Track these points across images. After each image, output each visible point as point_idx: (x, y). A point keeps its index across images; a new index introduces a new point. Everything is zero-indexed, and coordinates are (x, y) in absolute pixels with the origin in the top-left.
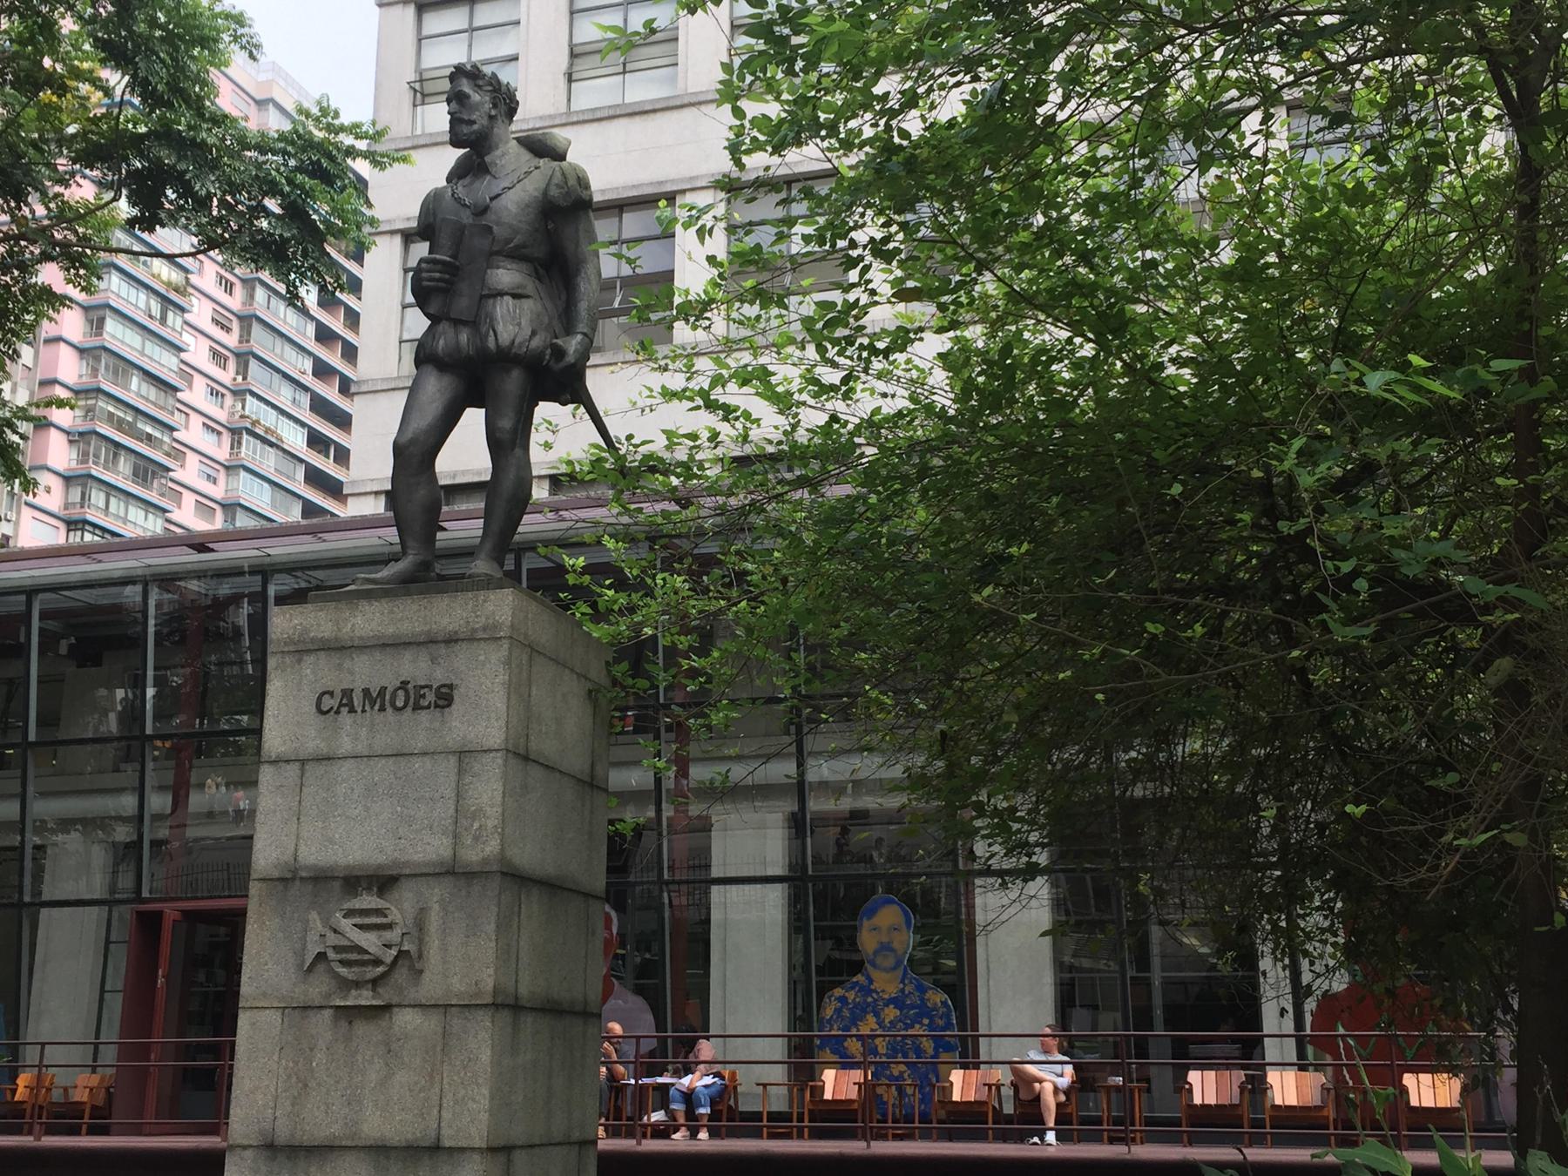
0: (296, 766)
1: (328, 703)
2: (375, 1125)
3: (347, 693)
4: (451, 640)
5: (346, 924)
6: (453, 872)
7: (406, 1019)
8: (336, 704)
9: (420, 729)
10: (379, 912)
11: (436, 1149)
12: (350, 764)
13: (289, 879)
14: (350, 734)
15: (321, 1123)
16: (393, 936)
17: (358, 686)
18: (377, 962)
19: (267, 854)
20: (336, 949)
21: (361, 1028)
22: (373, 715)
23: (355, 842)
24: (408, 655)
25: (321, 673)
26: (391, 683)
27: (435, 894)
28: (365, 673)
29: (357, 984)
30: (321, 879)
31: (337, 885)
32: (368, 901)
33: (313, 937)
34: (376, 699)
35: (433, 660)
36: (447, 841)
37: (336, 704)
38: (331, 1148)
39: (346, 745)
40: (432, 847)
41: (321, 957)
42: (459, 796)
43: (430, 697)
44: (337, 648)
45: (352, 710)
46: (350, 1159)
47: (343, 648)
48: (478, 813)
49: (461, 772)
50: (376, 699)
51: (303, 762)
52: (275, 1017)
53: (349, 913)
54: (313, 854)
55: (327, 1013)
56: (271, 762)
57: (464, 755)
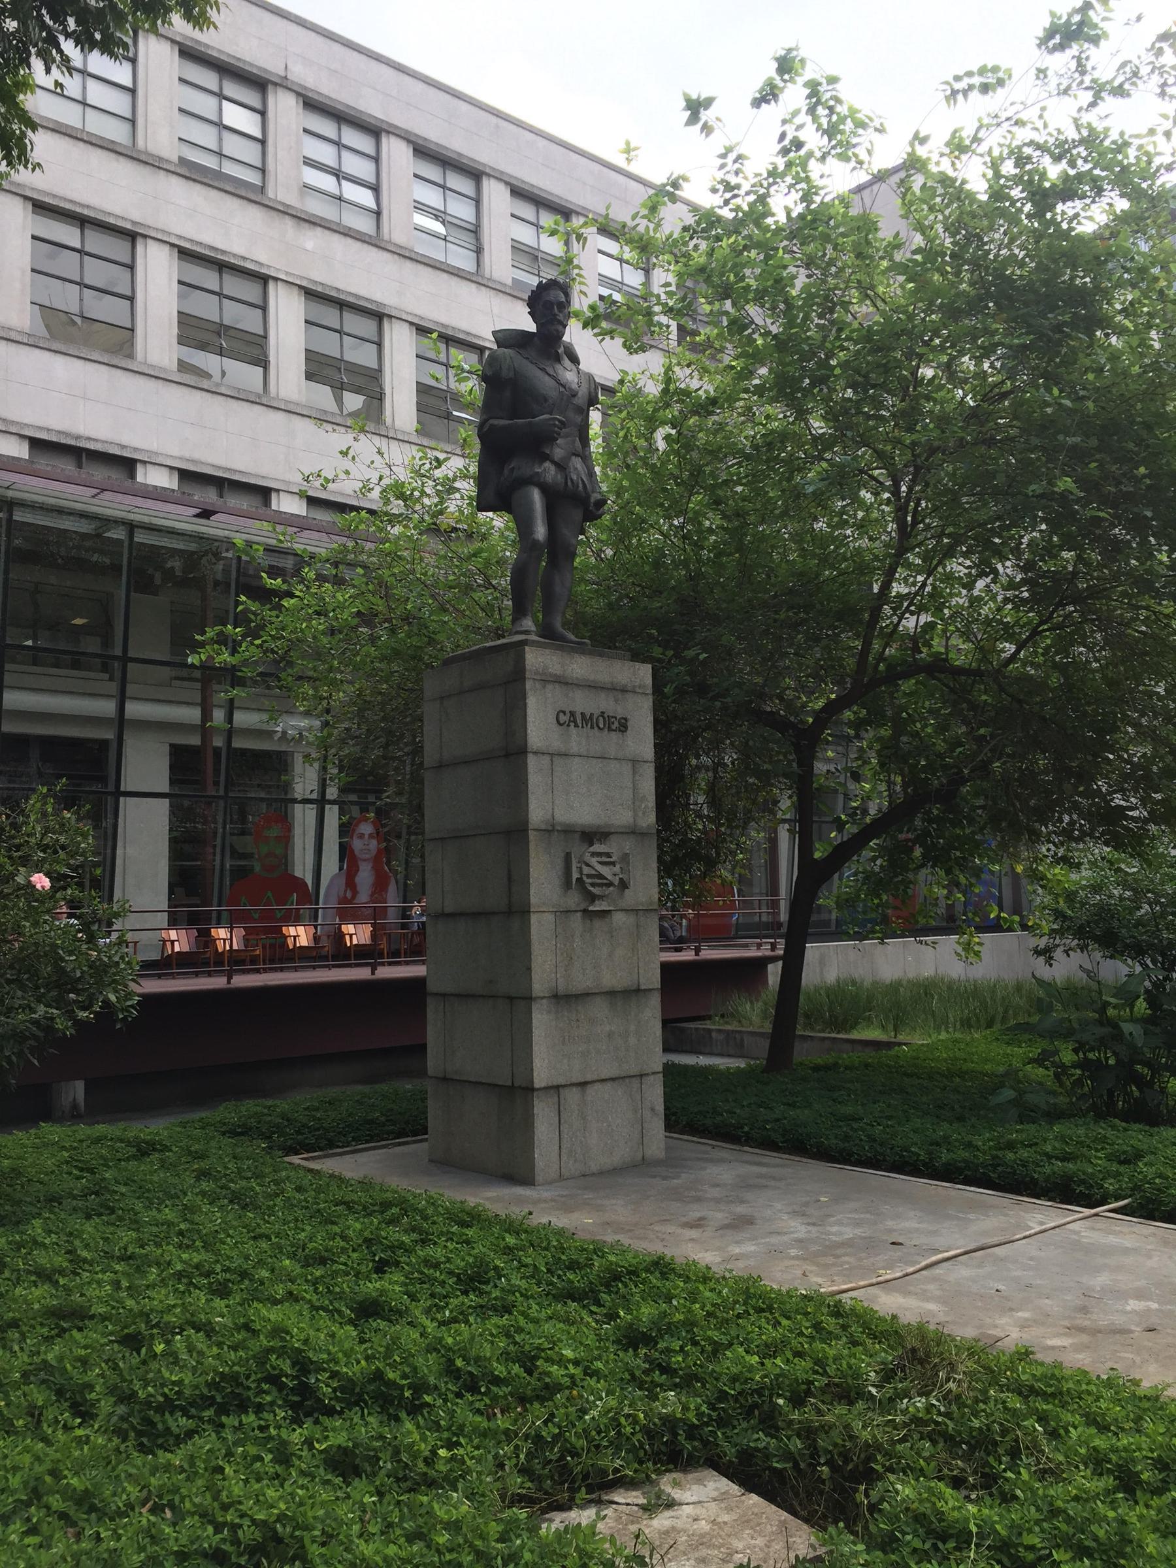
0: (547, 759)
1: (563, 718)
2: (610, 980)
3: (572, 714)
4: (624, 690)
5: (594, 861)
6: (633, 832)
7: (619, 918)
8: (568, 720)
9: (610, 742)
10: (608, 855)
11: (638, 991)
12: (577, 759)
13: (551, 830)
14: (577, 740)
15: (582, 981)
16: (617, 869)
17: (578, 710)
18: (610, 884)
19: (537, 813)
20: (589, 876)
21: (598, 923)
22: (587, 729)
23: (583, 810)
24: (603, 695)
25: (555, 698)
26: (596, 714)
27: (628, 845)
28: (582, 702)
29: (601, 897)
30: (568, 831)
31: (577, 836)
32: (597, 847)
33: (574, 869)
34: (588, 721)
35: (616, 701)
36: (631, 814)
37: (568, 720)
38: (588, 994)
39: (574, 748)
40: (622, 817)
41: (579, 880)
42: (635, 788)
43: (616, 724)
44: (562, 682)
45: (576, 726)
46: (598, 1000)
47: (567, 684)
48: (644, 798)
49: (634, 773)
50: (588, 721)
51: (552, 755)
52: (551, 917)
53: (593, 854)
54: (563, 816)
55: (579, 914)
56: (535, 753)
57: (635, 762)
